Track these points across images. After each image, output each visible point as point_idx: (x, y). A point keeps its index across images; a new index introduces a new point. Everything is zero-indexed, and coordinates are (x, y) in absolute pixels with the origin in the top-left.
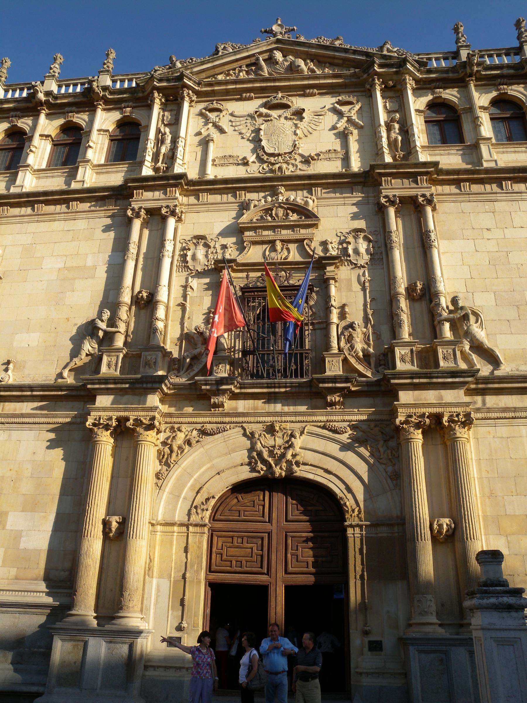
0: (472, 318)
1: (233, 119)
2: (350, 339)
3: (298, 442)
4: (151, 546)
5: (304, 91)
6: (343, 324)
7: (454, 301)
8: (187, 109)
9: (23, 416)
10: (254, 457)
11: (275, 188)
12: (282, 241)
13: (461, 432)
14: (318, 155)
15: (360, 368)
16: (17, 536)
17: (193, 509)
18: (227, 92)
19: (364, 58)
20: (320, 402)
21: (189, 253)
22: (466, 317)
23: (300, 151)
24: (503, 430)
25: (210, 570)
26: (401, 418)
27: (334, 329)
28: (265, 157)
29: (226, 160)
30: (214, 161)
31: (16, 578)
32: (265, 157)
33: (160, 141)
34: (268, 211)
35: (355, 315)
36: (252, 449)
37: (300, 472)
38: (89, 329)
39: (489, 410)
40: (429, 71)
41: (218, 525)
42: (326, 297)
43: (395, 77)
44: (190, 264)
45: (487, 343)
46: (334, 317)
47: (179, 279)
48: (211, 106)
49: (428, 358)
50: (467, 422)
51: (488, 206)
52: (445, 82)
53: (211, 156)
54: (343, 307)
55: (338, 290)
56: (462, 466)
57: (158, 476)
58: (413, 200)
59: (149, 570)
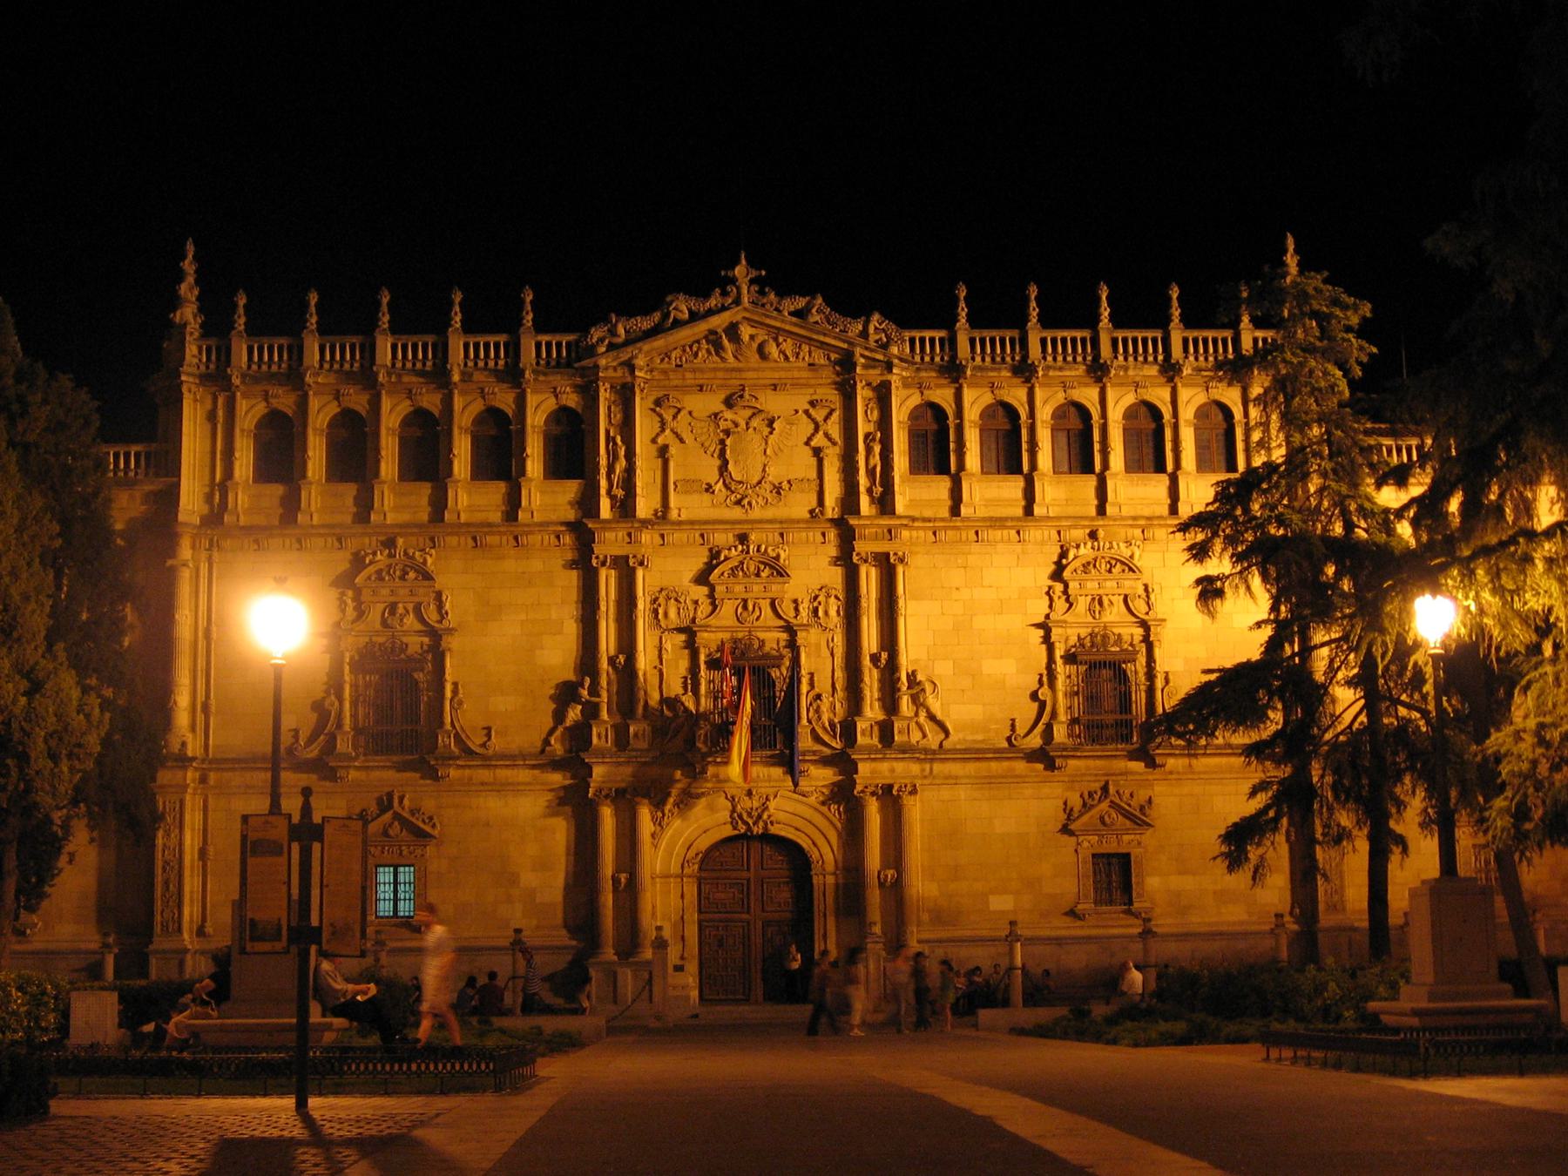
3: (772, 805)
10: (734, 821)
13: (908, 801)
15: (826, 738)
21: (661, 611)
25: (700, 912)
26: (859, 788)
31: (538, 927)
35: (823, 685)
36: (734, 810)
37: (774, 830)
38: (566, 694)
45: (939, 716)
46: (804, 688)
47: (653, 641)
49: (886, 731)
50: (914, 792)
54: (812, 675)
55: (808, 655)
56: (906, 828)
57: (653, 835)
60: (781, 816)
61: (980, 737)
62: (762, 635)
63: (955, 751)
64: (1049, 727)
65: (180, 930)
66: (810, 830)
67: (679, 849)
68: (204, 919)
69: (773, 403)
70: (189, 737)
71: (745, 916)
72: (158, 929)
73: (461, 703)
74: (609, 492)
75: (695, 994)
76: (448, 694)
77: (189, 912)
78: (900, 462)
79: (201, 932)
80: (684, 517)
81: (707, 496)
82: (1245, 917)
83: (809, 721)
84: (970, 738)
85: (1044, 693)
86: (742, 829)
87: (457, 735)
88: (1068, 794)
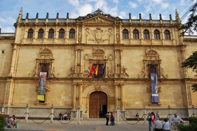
0: (126, 70)
2: (109, 72)
3: (101, 87)
4: (82, 100)
5: (103, 26)
7: (123, 67)
8: (83, 29)
9: (63, 82)
11: (98, 48)
12: (99, 56)
14: (105, 40)
15: (110, 77)
16: (63, 99)
17: (88, 95)
18: (90, 25)
19: (113, 21)
20: (104, 81)
22: (125, 70)
23: (102, 39)
24: (128, 86)
25: (90, 103)
27: (106, 70)
28: (96, 40)
29: (90, 40)
30: (88, 40)
31: (64, 105)
32: (96, 40)
33: (79, 35)
34: (97, 51)
39: (127, 83)
40: (124, 24)
41: (91, 97)
43: (118, 25)
44: (85, 59)
45: (127, 73)
48: (87, 28)
50: (123, 85)
51: (130, 51)
52: (127, 26)
53: (88, 39)
55: (107, 64)
57: (83, 91)
58: (119, 50)
59: (82, 103)
60: (103, 89)
61: (134, 77)
62: (100, 61)
63: (130, 79)
64: (144, 76)
65: (8, 104)
66: (107, 91)
67: (87, 93)
68: (13, 102)
69: (102, 28)
70: (13, 74)
71: (97, 104)
72: (4, 103)
73: (54, 70)
74: (78, 40)
75: (88, 116)
76: (52, 69)
77: (10, 101)
78: (121, 37)
79: (12, 105)
80: (89, 44)
81: (93, 42)
82: (175, 106)
83: (107, 74)
84: (132, 77)
85: (143, 70)
86: (96, 90)
87: (53, 75)
88: (147, 86)
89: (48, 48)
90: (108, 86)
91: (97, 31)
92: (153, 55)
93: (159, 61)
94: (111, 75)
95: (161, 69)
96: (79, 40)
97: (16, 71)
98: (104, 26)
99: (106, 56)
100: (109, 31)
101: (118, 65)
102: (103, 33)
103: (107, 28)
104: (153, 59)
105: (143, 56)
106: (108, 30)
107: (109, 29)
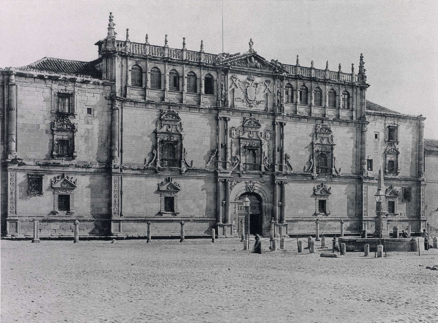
1: (240, 82)
6: (265, 157)
28: (248, 101)
32: (248, 101)
42: (261, 150)
69: (257, 80)
89: (173, 111)
90: (263, 184)
91: (249, 84)
92: (325, 136)
93: (332, 145)
94: (269, 165)
95: (334, 159)
96: (222, 99)
97: (122, 151)
98: (259, 75)
99: (261, 133)
100: (266, 86)
101: (278, 149)
102: (257, 89)
103: (263, 79)
104: (325, 142)
105: (312, 135)
106: (265, 84)
107: (266, 81)
